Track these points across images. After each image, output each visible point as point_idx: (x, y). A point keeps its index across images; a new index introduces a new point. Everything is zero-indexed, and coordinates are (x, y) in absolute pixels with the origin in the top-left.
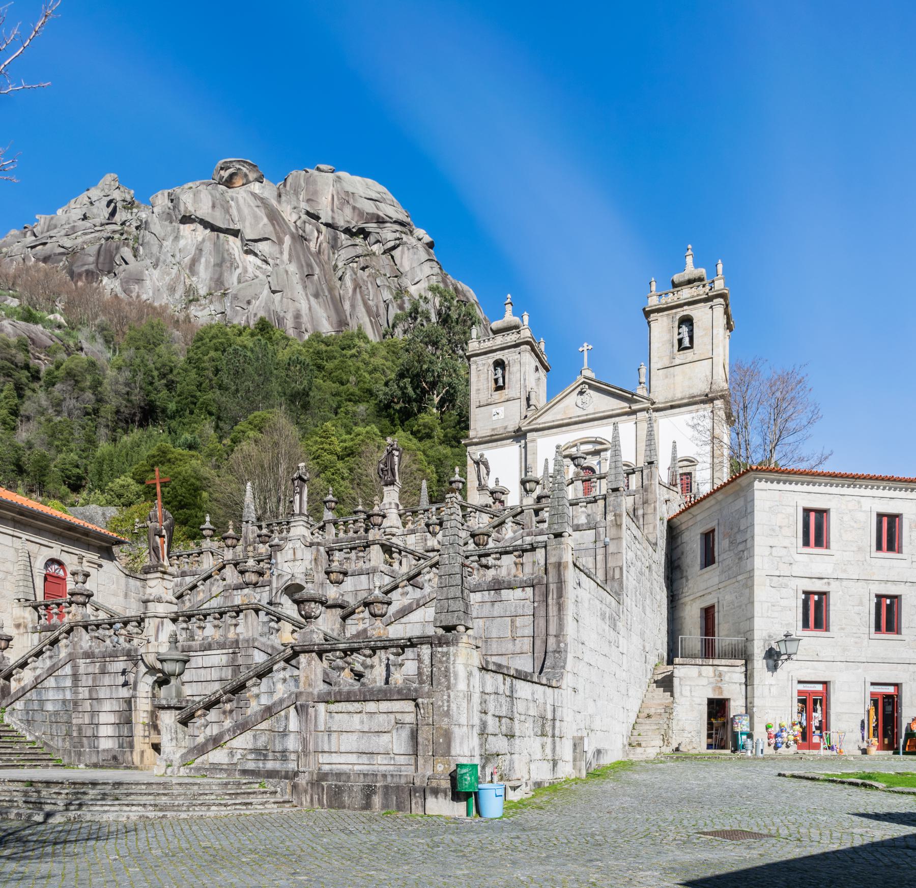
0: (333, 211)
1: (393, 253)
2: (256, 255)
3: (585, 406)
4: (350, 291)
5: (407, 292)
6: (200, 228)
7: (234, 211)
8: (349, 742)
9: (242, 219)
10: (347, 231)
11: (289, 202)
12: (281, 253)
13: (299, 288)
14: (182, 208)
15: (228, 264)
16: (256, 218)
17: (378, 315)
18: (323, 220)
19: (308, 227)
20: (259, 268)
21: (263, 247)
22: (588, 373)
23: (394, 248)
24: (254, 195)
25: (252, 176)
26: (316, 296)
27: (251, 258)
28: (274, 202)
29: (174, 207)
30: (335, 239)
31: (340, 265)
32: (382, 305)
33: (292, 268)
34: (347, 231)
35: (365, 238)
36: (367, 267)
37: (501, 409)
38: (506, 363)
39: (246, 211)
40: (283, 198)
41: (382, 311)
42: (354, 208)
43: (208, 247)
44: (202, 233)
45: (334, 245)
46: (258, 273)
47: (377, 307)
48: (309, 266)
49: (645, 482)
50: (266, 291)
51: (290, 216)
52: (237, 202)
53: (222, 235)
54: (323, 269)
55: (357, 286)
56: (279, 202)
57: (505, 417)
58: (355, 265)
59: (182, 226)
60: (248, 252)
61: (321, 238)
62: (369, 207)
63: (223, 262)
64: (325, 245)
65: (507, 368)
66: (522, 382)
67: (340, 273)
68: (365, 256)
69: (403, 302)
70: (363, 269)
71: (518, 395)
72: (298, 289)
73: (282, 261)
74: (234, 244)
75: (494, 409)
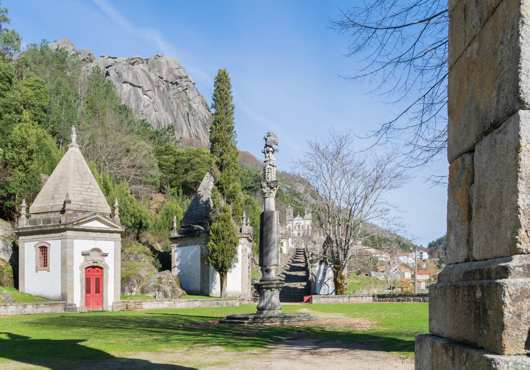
0: (167, 75)
1: (186, 91)
2: (147, 95)
5: (192, 107)
6: (129, 85)
7: (139, 79)
9: (142, 82)
10: (172, 83)
11: (153, 72)
12: (156, 95)
13: (162, 108)
14: (124, 78)
15: (140, 100)
16: (146, 81)
18: (164, 79)
19: (160, 82)
20: (148, 100)
21: (149, 93)
23: (186, 89)
24: (142, 69)
25: (141, 62)
26: (167, 111)
27: (145, 96)
28: (148, 72)
29: (119, 77)
30: (168, 86)
31: (171, 97)
33: (159, 101)
34: (172, 83)
35: (177, 85)
39: (142, 78)
40: (151, 71)
41: (186, 115)
42: (173, 74)
43: (132, 92)
44: (129, 87)
45: (168, 89)
46: (149, 103)
48: (163, 99)
50: (154, 111)
51: (154, 78)
52: (139, 75)
53: (136, 88)
54: (166, 99)
55: (178, 107)
56: (149, 72)
59: (123, 84)
60: (144, 94)
61: (164, 86)
62: (176, 72)
63: (138, 99)
64: (165, 89)
67: (172, 100)
72: (163, 111)
73: (156, 98)
74: (140, 90)
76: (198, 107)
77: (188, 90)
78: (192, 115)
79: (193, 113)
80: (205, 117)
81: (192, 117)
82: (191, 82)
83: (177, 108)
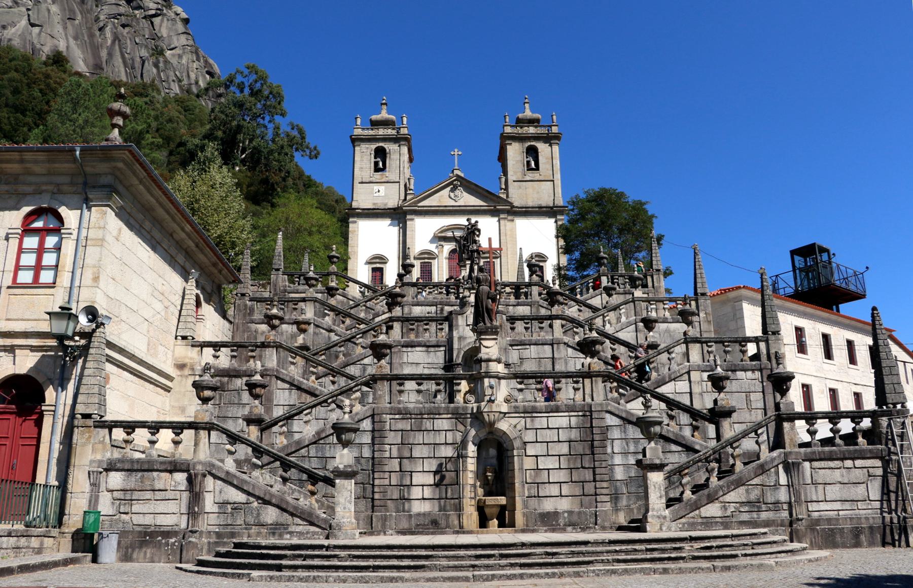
3: (457, 199)
4: (109, 42)
8: (833, 492)
17: (133, 68)
22: (456, 172)
31: (102, 17)
32: (138, 59)
36: (128, 25)
37: (382, 188)
38: (388, 151)
47: (133, 60)
49: (656, 284)
55: (116, 38)
57: (386, 195)
58: (116, 21)
65: (388, 155)
66: (401, 169)
67: (101, 24)
68: (127, 16)
69: (158, 62)
70: (124, 26)
71: (397, 180)
75: (376, 187)
76: (180, 56)
77: (160, 18)
78: (156, 65)
79: (161, 65)
80: (197, 83)
81: (155, 70)
82: (177, 15)
83: (113, 42)
